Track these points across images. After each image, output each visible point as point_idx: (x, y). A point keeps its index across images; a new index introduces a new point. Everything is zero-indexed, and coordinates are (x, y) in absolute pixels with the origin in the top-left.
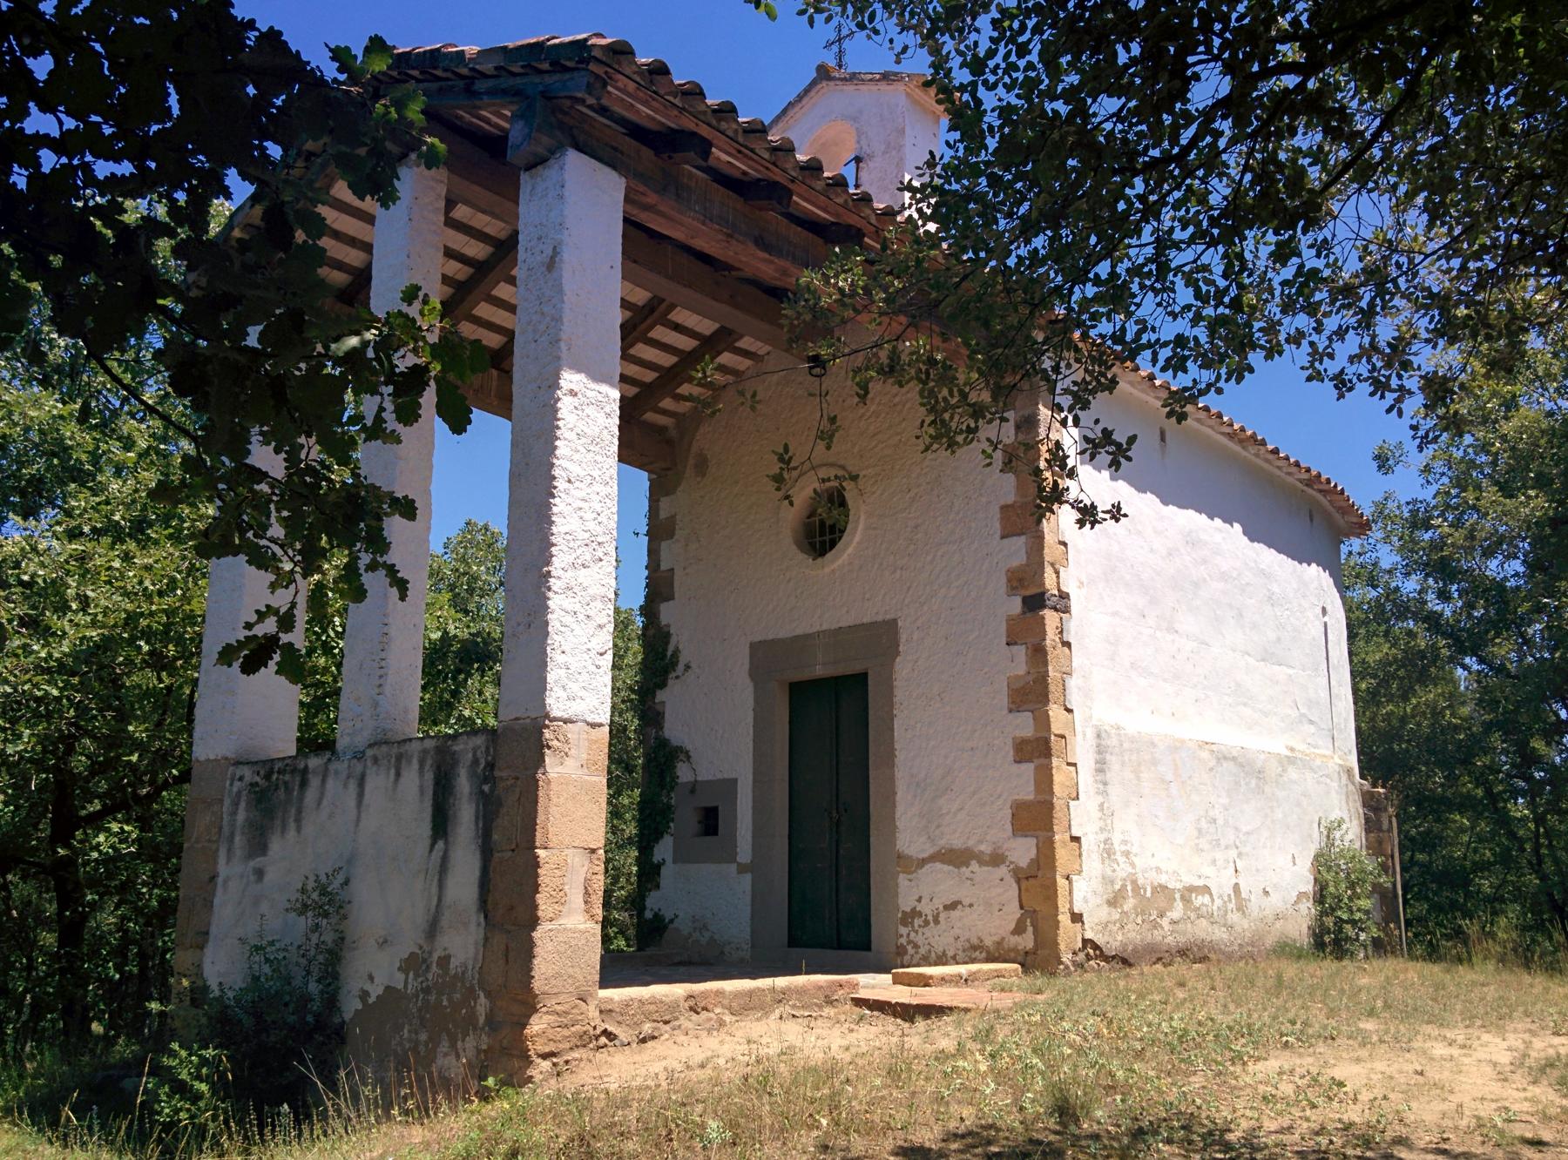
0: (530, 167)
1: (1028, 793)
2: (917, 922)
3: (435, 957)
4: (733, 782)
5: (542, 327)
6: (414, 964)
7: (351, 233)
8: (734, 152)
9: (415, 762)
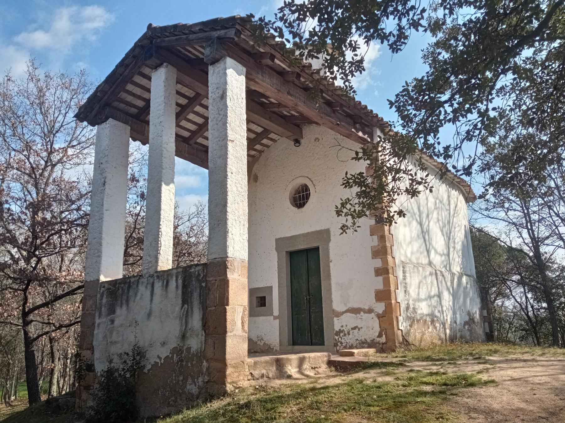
0: (213, 63)
1: (381, 287)
2: (341, 335)
3: (185, 347)
4: (271, 288)
5: (219, 119)
6: (177, 351)
7: (139, 94)
8: (282, 60)
9: (174, 278)
